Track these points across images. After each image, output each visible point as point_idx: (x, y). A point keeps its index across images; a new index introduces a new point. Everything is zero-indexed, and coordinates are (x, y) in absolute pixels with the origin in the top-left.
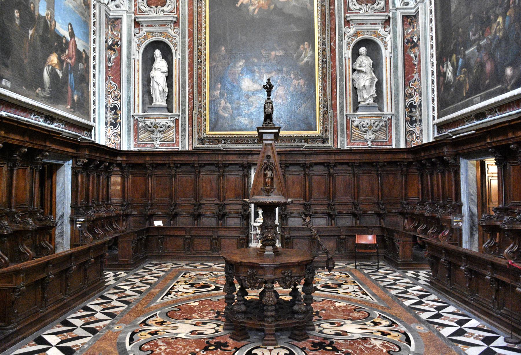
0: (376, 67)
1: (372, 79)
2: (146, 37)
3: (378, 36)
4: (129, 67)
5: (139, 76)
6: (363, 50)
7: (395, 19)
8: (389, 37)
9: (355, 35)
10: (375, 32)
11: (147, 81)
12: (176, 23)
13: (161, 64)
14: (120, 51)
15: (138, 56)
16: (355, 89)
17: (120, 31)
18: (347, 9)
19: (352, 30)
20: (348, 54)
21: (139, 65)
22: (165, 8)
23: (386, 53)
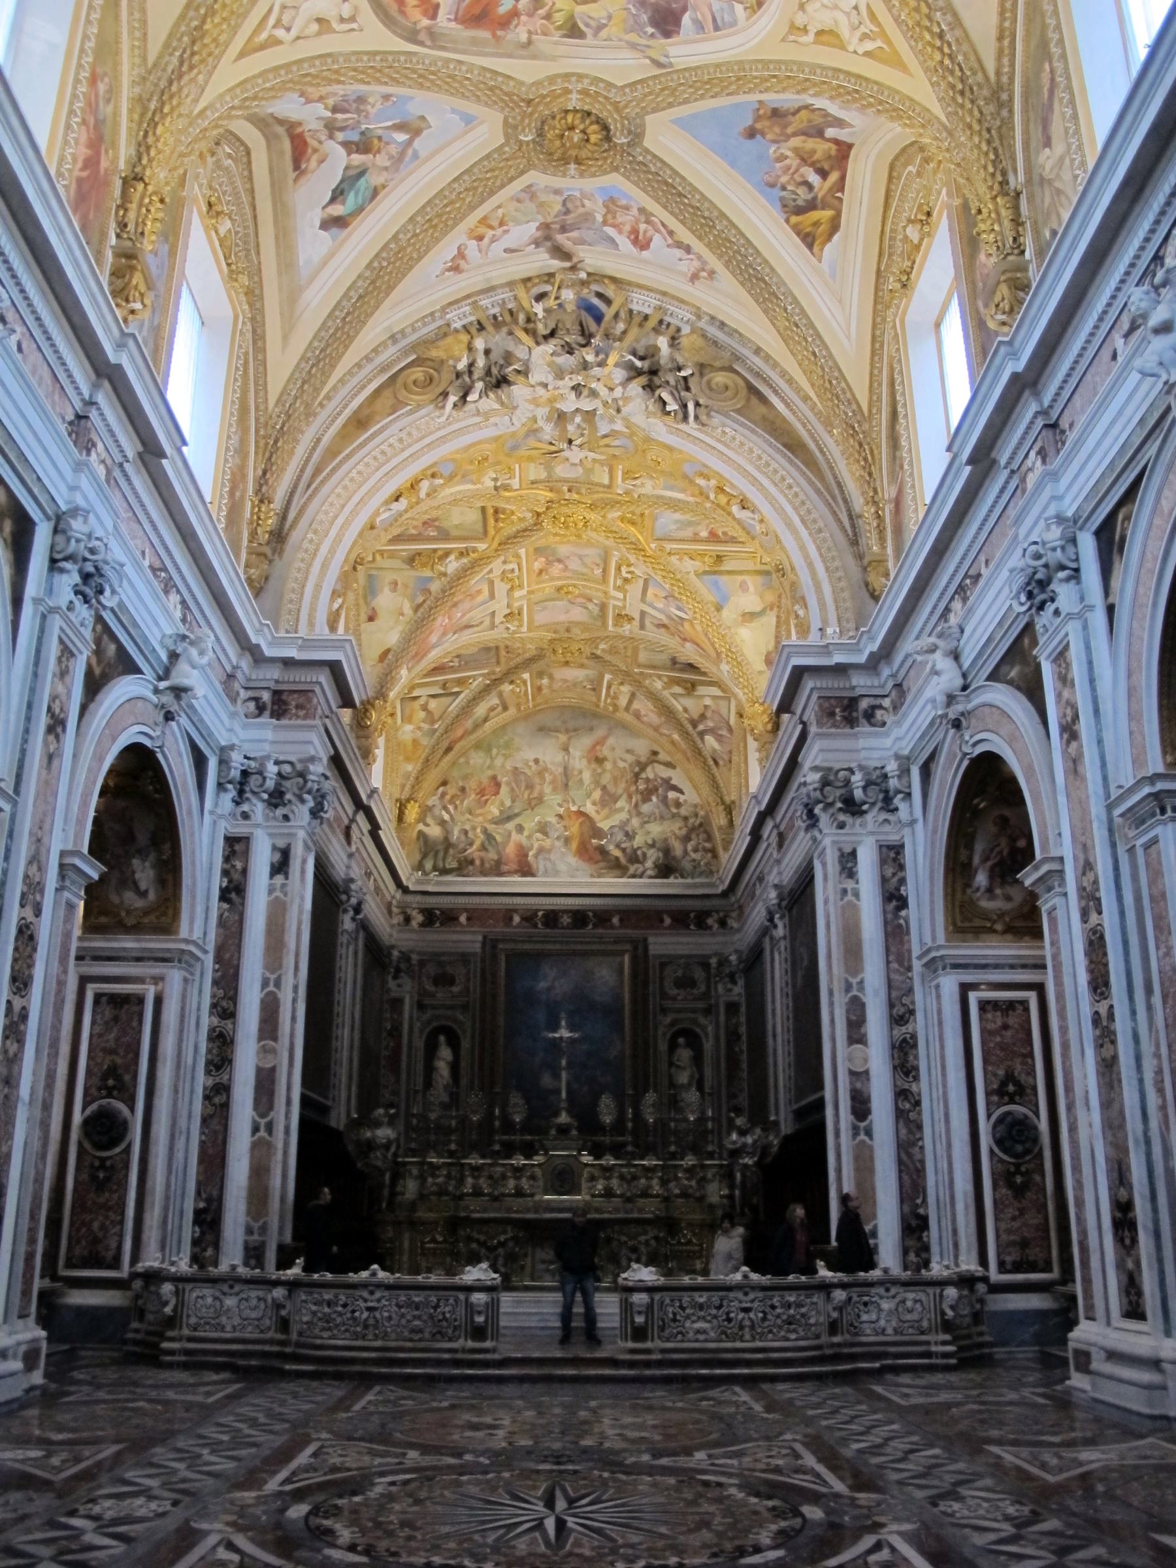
0: (698, 1059)
1: (692, 1077)
2: (429, 1022)
3: (699, 1025)
4: (409, 1056)
5: (420, 1067)
6: (681, 1040)
7: (717, 1005)
8: (710, 1029)
9: (672, 1024)
10: (695, 1021)
11: (429, 1069)
12: (465, 1007)
13: (445, 1053)
14: (400, 1036)
15: (420, 1043)
16: (672, 1084)
17: (401, 1014)
18: (664, 995)
19: (668, 1020)
20: (663, 1047)
21: (421, 1054)
22: (455, 989)
23: (708, 1046)
